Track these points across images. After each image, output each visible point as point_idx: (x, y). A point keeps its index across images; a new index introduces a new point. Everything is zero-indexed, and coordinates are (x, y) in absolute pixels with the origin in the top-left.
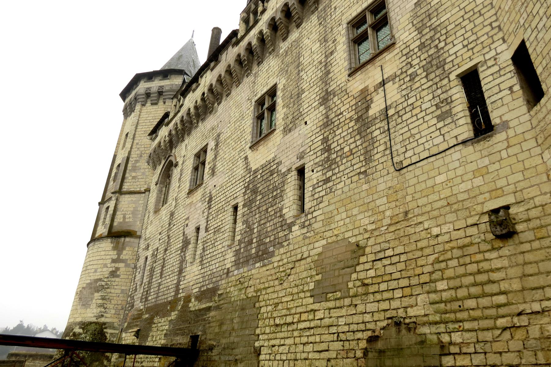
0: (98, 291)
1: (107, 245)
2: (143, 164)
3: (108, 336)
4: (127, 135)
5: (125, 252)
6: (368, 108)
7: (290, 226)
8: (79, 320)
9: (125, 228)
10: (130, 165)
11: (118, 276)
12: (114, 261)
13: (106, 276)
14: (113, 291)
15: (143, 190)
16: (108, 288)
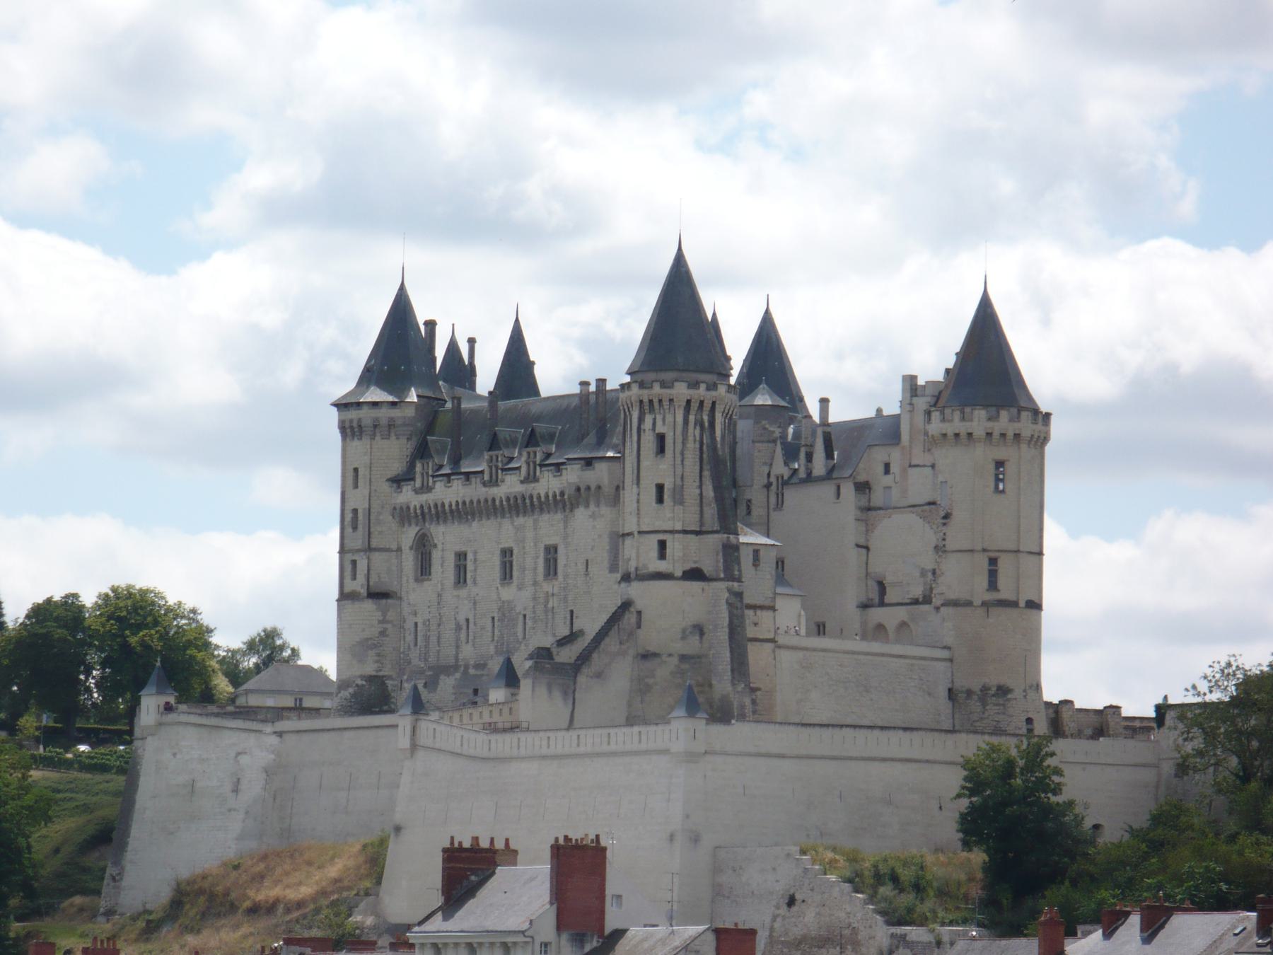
0: (372, 649)
1: (369, 605)
2: (387, 517)
3: (389, 685)
4: (356, 470)
5: (389, 614)
6: (548, 604)
7: (521, 643)
8: (358, 673)
9: (383, 589)
10: (372, 517)
11: (387, 636)
12: (380, 622)
13: (377, 635)
14: (385, 649)
15: (394, 547)
16: (381, 646)
